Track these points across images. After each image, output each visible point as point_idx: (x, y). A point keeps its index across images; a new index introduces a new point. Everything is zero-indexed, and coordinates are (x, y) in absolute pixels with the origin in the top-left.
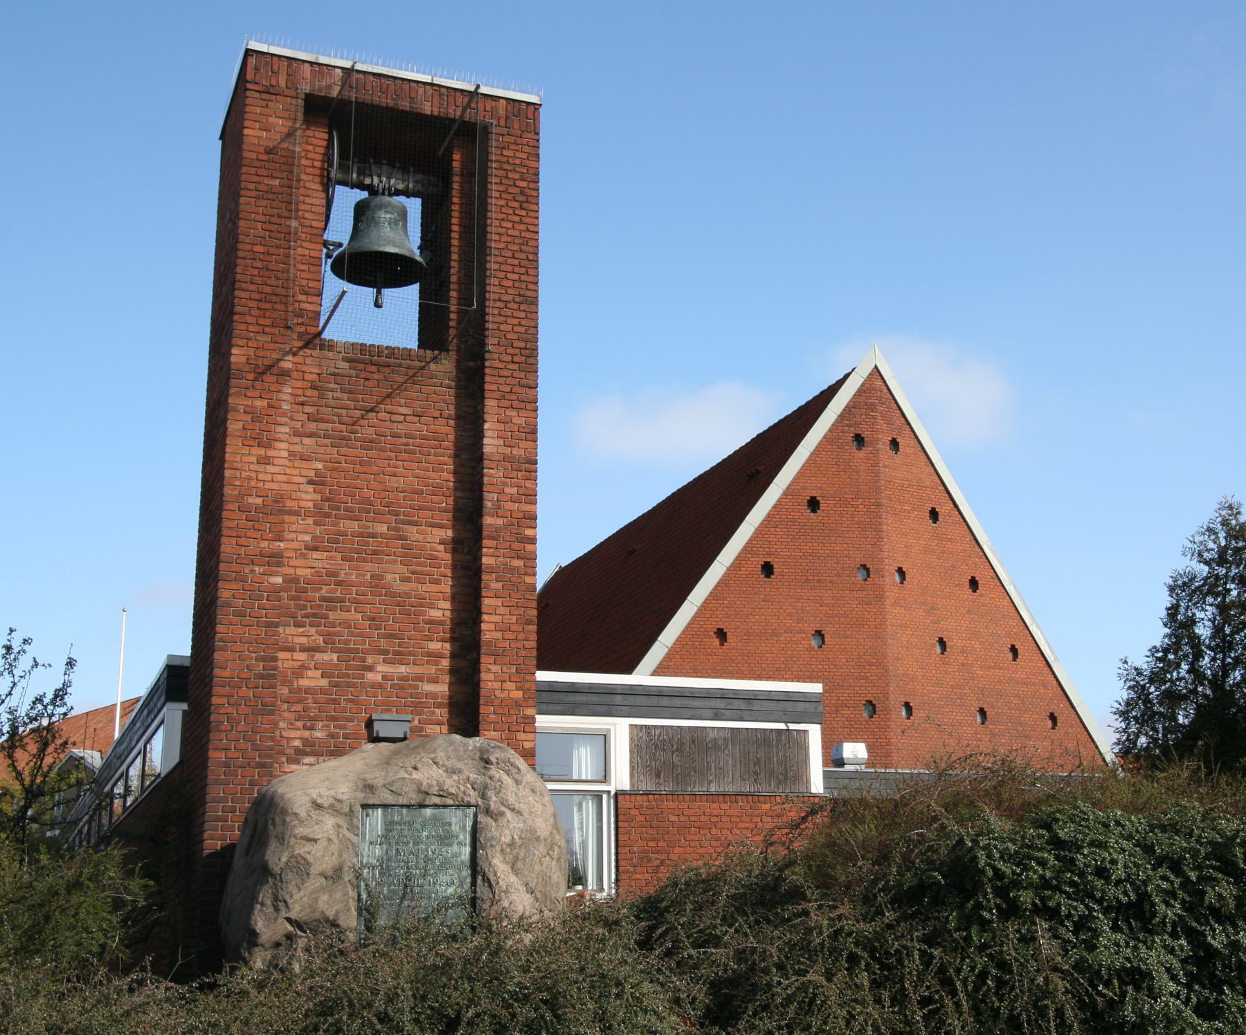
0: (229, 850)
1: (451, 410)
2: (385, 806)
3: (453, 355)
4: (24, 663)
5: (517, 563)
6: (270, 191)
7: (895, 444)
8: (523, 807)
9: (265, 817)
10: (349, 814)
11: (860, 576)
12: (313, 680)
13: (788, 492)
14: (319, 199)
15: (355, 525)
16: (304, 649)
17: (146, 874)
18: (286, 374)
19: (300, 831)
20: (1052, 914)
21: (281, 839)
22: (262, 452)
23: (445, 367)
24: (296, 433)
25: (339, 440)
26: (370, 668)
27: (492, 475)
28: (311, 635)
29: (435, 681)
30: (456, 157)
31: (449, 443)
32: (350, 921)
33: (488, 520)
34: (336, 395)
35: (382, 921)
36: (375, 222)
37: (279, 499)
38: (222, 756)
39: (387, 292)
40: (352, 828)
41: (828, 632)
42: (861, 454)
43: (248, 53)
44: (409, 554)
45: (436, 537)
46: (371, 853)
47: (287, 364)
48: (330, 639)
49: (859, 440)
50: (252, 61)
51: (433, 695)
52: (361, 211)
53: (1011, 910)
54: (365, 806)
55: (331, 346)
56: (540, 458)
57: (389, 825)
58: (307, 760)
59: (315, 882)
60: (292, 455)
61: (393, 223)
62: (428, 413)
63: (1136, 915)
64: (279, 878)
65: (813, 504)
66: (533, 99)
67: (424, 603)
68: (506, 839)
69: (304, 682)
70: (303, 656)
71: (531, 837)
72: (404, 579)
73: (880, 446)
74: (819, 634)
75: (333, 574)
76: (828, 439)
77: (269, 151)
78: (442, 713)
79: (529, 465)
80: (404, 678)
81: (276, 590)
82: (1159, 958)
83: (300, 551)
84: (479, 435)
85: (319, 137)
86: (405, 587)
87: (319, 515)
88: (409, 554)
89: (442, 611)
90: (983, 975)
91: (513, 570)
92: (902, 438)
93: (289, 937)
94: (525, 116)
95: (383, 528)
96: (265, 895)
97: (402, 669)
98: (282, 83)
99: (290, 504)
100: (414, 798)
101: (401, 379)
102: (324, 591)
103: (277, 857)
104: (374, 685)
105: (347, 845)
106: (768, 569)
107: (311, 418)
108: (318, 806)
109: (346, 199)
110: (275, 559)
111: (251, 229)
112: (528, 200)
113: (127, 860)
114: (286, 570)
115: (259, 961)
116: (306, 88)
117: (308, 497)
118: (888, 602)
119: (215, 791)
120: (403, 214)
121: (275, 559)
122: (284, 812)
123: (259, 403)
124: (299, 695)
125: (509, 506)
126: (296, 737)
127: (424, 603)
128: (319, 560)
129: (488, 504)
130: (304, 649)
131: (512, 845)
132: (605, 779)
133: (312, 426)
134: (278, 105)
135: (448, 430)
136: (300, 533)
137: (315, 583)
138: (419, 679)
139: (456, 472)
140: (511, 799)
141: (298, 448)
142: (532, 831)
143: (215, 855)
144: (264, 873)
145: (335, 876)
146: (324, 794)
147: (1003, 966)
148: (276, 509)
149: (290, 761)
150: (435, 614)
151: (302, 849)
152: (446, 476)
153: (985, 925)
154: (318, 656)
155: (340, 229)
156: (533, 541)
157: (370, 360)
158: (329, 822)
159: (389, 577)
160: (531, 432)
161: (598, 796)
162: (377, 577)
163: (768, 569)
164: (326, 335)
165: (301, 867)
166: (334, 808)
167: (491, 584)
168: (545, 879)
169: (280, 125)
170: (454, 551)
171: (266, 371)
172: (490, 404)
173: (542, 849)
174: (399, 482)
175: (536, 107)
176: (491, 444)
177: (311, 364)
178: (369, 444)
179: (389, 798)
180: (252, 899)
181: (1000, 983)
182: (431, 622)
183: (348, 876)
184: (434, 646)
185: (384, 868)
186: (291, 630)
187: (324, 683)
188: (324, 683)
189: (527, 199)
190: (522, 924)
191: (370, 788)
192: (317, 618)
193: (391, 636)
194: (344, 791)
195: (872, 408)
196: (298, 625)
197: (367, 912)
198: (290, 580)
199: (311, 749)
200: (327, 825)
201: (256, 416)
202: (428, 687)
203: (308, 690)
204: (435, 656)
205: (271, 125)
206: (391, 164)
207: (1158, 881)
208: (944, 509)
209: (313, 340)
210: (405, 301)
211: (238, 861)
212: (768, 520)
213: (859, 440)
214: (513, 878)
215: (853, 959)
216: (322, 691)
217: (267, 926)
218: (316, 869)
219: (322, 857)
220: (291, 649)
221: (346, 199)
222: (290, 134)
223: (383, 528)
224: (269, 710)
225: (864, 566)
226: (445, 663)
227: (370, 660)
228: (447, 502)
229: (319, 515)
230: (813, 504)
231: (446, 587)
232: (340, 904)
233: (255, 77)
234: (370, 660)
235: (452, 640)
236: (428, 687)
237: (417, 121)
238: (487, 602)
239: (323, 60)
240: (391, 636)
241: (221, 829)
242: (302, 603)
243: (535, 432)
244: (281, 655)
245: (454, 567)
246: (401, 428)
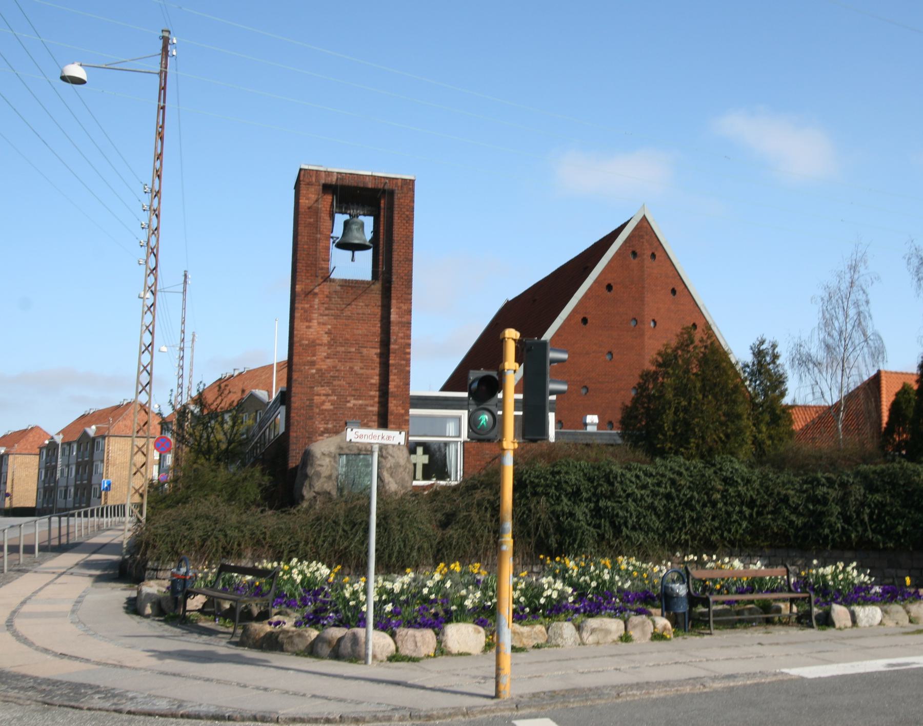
0: (297, 467)
1: (379, 303)
2: (347, 455)
3: (380, 282)
4: (226, 392)
5: (403, 362)
6: (310, 223)
7: (653, 256)
8: (395, 455)
9: (307, 456)
10: (335, 457)
11: (633, 323)
12: (328, 406)
13: (596, 282)
14: (329, 223)
15: (343, 349)
16: (324, 395)
17: (270, 474)
18: (316, 294)
19: (318, 462)
20: (547, 494)
21: (312, 465)
22: (307, 324)
23: (378, 286)
24: (321, 315)
25: (337, 317)
26: (349, 402)
27: (394, 329)
28: (327, 390)
29: (372, 406)
30: (382, 202)
31: (379, 316)
32: (334, 493)
33: (392, 346)
34: (335, 299)
35: (345, 492)
36: (350, 229)
37: (314, 341)
38: (295, 434)
39: (356, 253)
40: (335, 462)
41: (615, 351)
42: (636, 261)
43: (301, 170)
44: (363, 359)
45: (373, 352)
46: (342, 470)
47: (316, 290)
48: (334, 392)
49: (634, 254)
50: (302, 172)
51: (372, 411)
52: (346, 224)
53: (535, 494)
54: (340, 455)
55: (333, 281)
56: (413, 322)
57: (348, 461)
58: (326, 435)
59: (322, 480)
60: (319, 323)
61: (358, 230)
62: (371, 306)
63: (575, 495)
64: (311, 478)
65: (609, 287)
66: (412, 178)
67: (369, 377)
68: (388, 466)
69: (324, 407)
70: (324, 398)
71: (397, 465)
72: (361, 368)
73: (645, 256)
74: (610, 353)
75: (335, 367)
76: (618, 254)
77: (309, 208)
78: (375, 418)
79: (408, 324)
80: (361, 405)
81: (313, 375)
82: (582, 511)
83: (322, 359)
84: (389, 314)
85: (329, 198)
86: (362, 371)
87: (330, 345)
88: (363, 359)
89: (375, 380)
90: (524, 513)
91: (401, 365)
92: (657, 252)
93: (315, 497)
94: (409, 185)
95: (353, 350)
96: (307, 483)
97: (361, 402)
98: (314, 179)
99: (318, 342)
100: (356, 451)
101: (360, 292)
102: (332, 374)
103: (310, 471)
104: (350, 408)
105: (333, 467)
106: (585, 321)
107: (326, 309)
108: (323, 454)
109: (340, 219)
110: (313, 363)
111: (303, 239)
112: (409, 219)
113: (263, 470)
114: (317, 366)
115: (305, 505)
116: (323, 181)
117: (325, 339)
118: (646, 337)
119: (292, 447)
120: (362, 225)
121: (313, 363)
122: (313, 456)
123: (307, 306)
124: (322, 412)
125: (400, 341)
126: (322, 427)
127: (369, 377)
128: (329, 362)
129: (392, 340)
130: (324, 395)
131: (391, 467)
132: (459, 436)
133: (327, 312)
134: (312, 189)
135: (378, 311)
136: (322, 352)
137: (329, 370)
138: (367, 405)
139: (381, 327)
140: (391, 452)
141: (321, 321)
142: (398, 463)
143: (293, 469)
144: (306, 476)
145: (329, 477)
146: (325, 450)
147: (530, 511)
148: (313, 345)
149: (320, 435)
150: (373, 381)
151: (319, 469)
152: (377, 329)
153: (528, 498)
154: (330, 398)
155: (338, 231)
156: (409, 353)
157: (350, 286)
158: (327, 460)
159: (356, 368)
160: (409, 312)
161: (457, 442)
162: (351, 368)
163: (585, 321)
164: (332, 276)
165: (318, 475)
166: (329, 455)
167: (393, 370)
168: (403, 479)
169: (313, 197)
170: (380, 357)
171: (309, 293)
172: (394, 302)
173: (402, 469)
174: (360, 332)
175: (413, 181)
176: (393, 317)
177: (326, 288)
178: (348, 318)
179: (348, 452)
180: (302, 485)
181: (528, 516)
182: (371, 384)
183: (334, 478)
184: (372, 393)
185: (346, 475)
186: (319, 388)
187: (331, 407)
188: (331, 407)
189: (409, 219)
190: (396, 493)
191: (341, 448)
192: (329, 384)
193: (356, 390)
194: (333, 449)
195: (642, 237)
196: (322, 386)
197: (340, 490)
198: (319, 370)
199: (326, 431)
200: (326, 461)
201: (306, 311)
202: (370, 409)
203: (326, 410)
204: (372, 397)
205: (311, 196)
206: (358, 204)
207: (585, 485)
208: (679, 289)
209: (327, 279)
210: (365, 258)
211: (299, 472)
212: (586, 296)
213: (634, 254)
214: (391, 479)
215: (486, 509)
216: (331, 410)
217: (307, 493)
218: (323, 475)
219: (325, 471)
220: (319, 395)
221: (340, 219)
222: (317, 201)
223: (353, 350)
224: (311, 418)
225: (635, 319)
226: (377, 399)
227: (348, 399)
228: (377, 339)
229: (330, 345)
230: (609, 287)
231: (377, 371)
232: (330, 487)
233: (303, 180)
234: (348, 399)
235: (379, 391)
236: (370, 409)
237: (365, 190)
238: (391, 377)
239: (329, 170)
240: (356, 390)
241: (294, 461)
242: (323, 378)
243: (410, 311)
244: (316, 397)
245: (380, 363)
246: (360, 311)
